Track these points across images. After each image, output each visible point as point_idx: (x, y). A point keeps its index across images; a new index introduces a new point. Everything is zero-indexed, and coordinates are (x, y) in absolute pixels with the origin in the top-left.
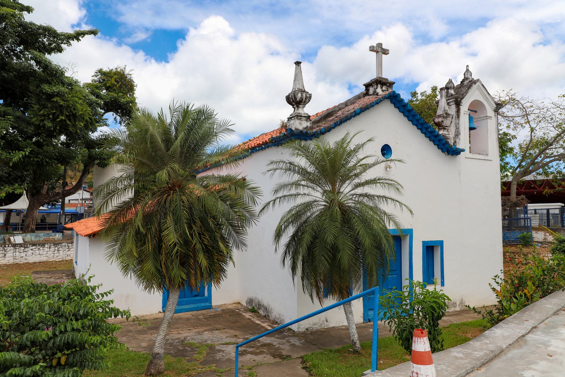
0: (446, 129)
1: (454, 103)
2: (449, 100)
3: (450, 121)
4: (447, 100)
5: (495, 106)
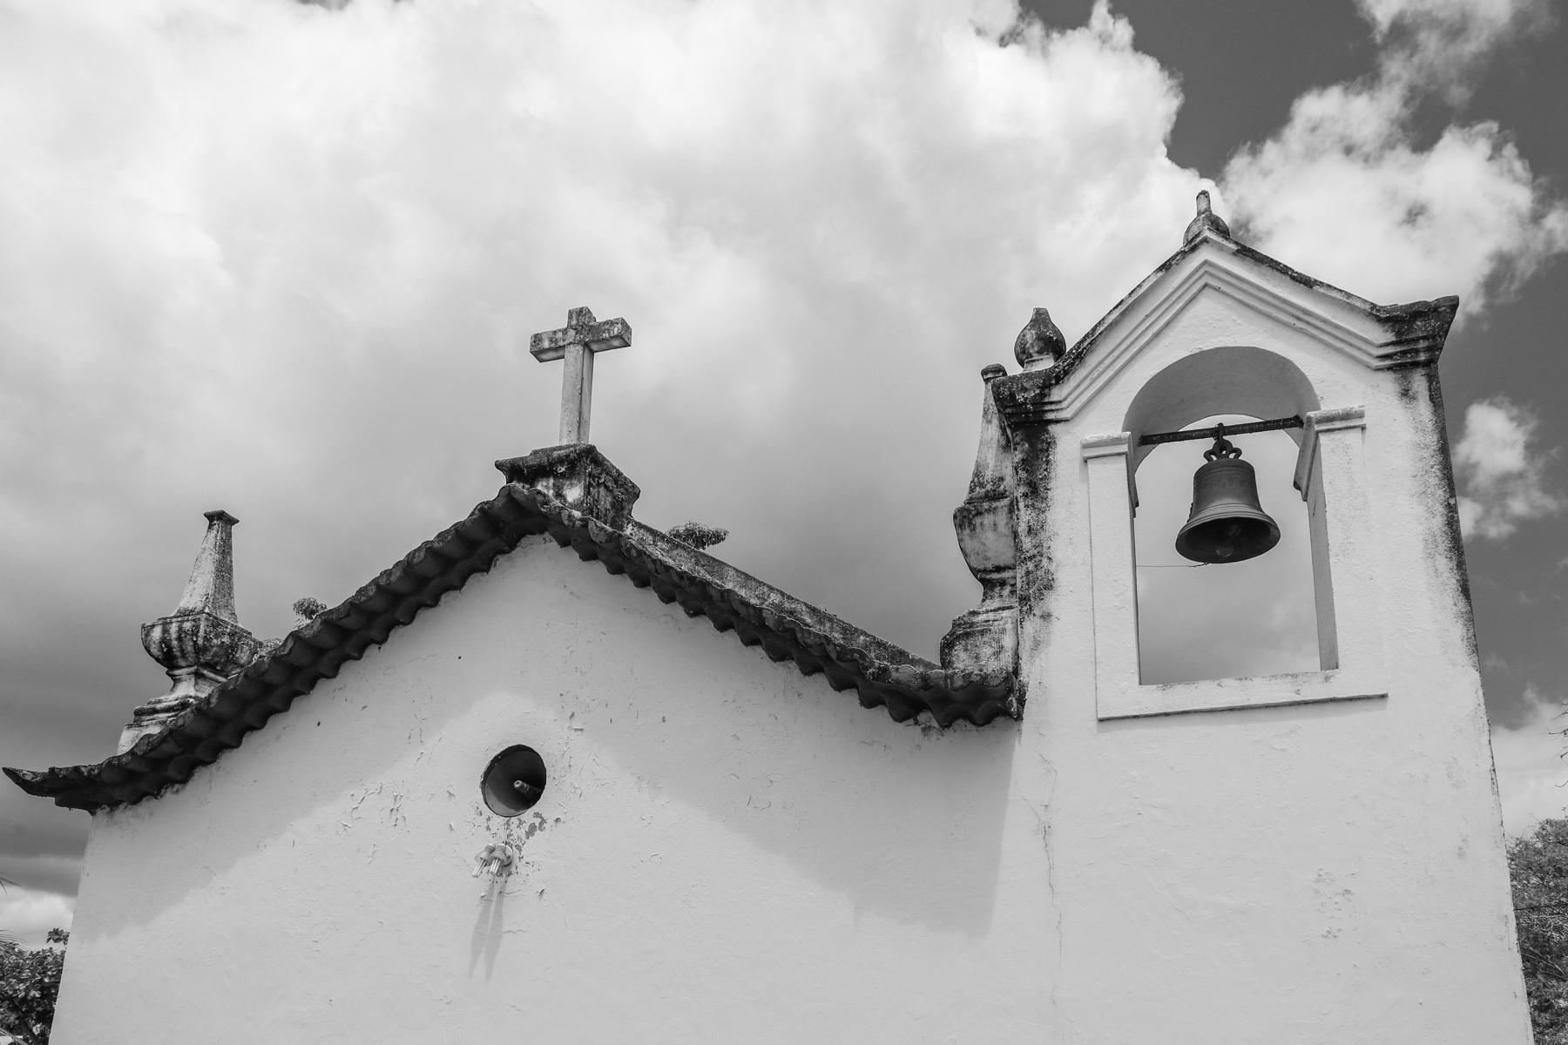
0: (1003, 583)
5: (1379, 335)
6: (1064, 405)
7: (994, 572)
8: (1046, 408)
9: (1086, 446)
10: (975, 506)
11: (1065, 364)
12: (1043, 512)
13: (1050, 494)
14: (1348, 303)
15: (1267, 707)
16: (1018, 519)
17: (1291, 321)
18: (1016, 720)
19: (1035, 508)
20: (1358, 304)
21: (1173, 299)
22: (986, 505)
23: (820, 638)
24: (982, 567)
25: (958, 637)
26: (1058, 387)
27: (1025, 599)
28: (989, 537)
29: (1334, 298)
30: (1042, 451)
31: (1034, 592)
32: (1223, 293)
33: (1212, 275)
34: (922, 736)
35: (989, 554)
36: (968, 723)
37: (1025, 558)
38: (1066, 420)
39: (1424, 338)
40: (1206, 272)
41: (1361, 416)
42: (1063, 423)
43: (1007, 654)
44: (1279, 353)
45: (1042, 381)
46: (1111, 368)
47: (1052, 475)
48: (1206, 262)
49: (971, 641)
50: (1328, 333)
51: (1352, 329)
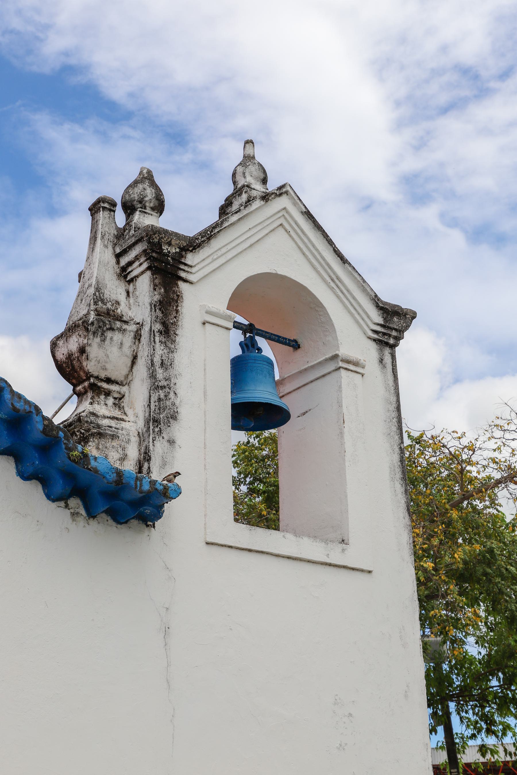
0: (108, 394)
1: (145, 265)
2: (124, 252)
3: (127, 350)
4: (118, 256)
5: (377, 317)
6: (193, 270)
7: (105, 381)
8: (182, 267)
9: (208, 312)
10: (110, 321)
11: (203, 239)
12: (172, 352)
13: (178, 339)
14: (363, 286)
15: (309, 561)
16: (154, 350)
17: (329, 280)
18: (147, 526)
19: (166, 346)
20: (368, 289)
22: (118, 324)
23: (30, 407)
24: (96, 374)
25: (93, 435)
26: (191, 253)
27: (157, 421)
28: (113, 352)
29: (356, 278)
30: (173, 299)
31: (163, 417)
32: (290, 236)
33: (286, 219)
34: (71, 521)
35: (108, 366)
36: (109, 518)
37: (158, 386)
38: (191, 283)
39: (396, 330)
40: (283, 215)
41: (363, 367)
42: (188, 283)
43: (130, 463)
44: (320, 300)
45: (185, 244)
46: (224, 257)
47: (180, 323)
48: (285, 209)
49: (102, 441)
50: (348, 299)
51: (362, 304)
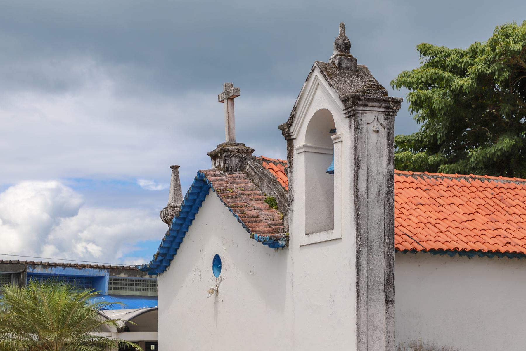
21: (311, 90)
